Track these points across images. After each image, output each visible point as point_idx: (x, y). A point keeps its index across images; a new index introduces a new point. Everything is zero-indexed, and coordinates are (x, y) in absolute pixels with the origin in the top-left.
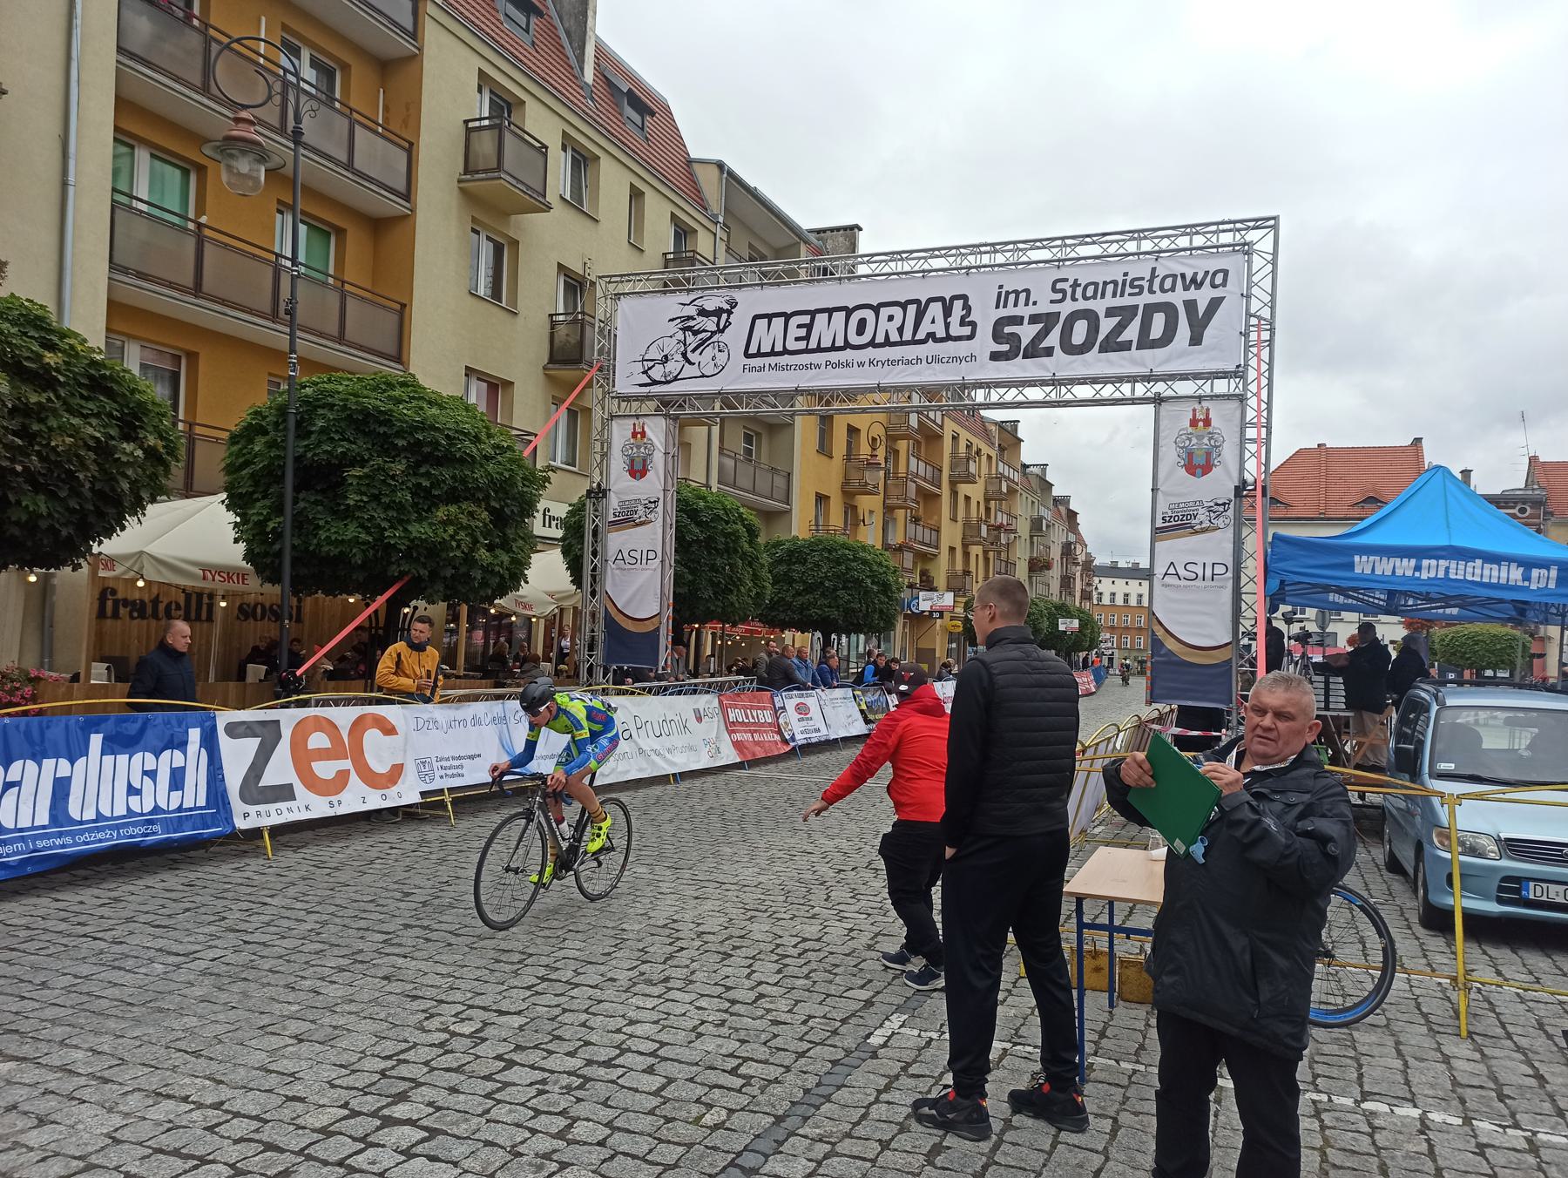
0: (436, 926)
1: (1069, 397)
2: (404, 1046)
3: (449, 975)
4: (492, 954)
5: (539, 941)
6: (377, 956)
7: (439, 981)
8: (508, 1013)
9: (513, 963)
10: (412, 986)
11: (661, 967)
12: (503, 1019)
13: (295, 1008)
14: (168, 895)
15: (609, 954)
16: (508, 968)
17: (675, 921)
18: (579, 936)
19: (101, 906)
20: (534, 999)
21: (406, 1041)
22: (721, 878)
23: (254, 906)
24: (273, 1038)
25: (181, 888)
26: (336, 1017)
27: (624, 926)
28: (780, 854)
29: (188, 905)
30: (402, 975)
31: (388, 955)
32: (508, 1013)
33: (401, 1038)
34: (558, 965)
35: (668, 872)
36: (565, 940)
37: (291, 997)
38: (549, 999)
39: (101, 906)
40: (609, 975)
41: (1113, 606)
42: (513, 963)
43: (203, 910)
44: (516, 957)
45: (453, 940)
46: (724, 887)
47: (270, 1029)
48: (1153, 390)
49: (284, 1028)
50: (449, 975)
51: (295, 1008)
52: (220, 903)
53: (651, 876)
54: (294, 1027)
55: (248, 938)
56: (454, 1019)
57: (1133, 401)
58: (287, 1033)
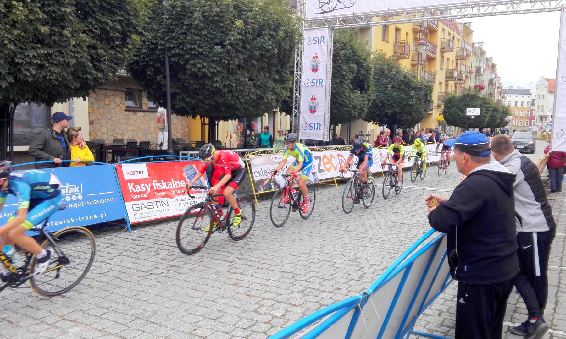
0: (251, 259)
1: (518, 9)
2: (252, 323)
3: (263, 284)
4: (279, 274)
5: (298, 267)
6: (229, 273)
7: (260, 287)
8: (295, 305)
9: (290, 278)
10: (248, 290)
11: (359, 283)
12: (294, 309)
13: (198, 300)
14: (134, 242)
15: (332, 275)
16: (288, 281)
17: (357, 258)
18: (316, 265)
19: (107, 247)
20: (305, 298)
21: (252, 320)
22: (370, 236)
23: (171, 248)
24: (193, 317)
25: (139, 239)
26: (218, 305)
27: (334, 260)
28: (392, 225)
29: (143, 247)
30: (241, 283)
31: (233, 273)
32: (295, 305)
33: (250, 318)
34: (309, 280)
35: (344, 233)
36: (310, 267)
37: (196, 294)
38: (311, 298)
39: (107, 247)
40: (336, 286)
41: (522, 107)
42: (290, 278)
43: (150, 249)
44: (291, 276)
45: (260, 266)
46: (373, 241)
47: (190, 311)
48: (561, 4)
49: (197, 311)
50: (263, 284)
51: (198, 300)
52: (156, 246)
53: (338, 235)
54: (201, 311)
55: (171, 263)
56: (271, 308)
57: (550, 10)
58: (198, 314)
